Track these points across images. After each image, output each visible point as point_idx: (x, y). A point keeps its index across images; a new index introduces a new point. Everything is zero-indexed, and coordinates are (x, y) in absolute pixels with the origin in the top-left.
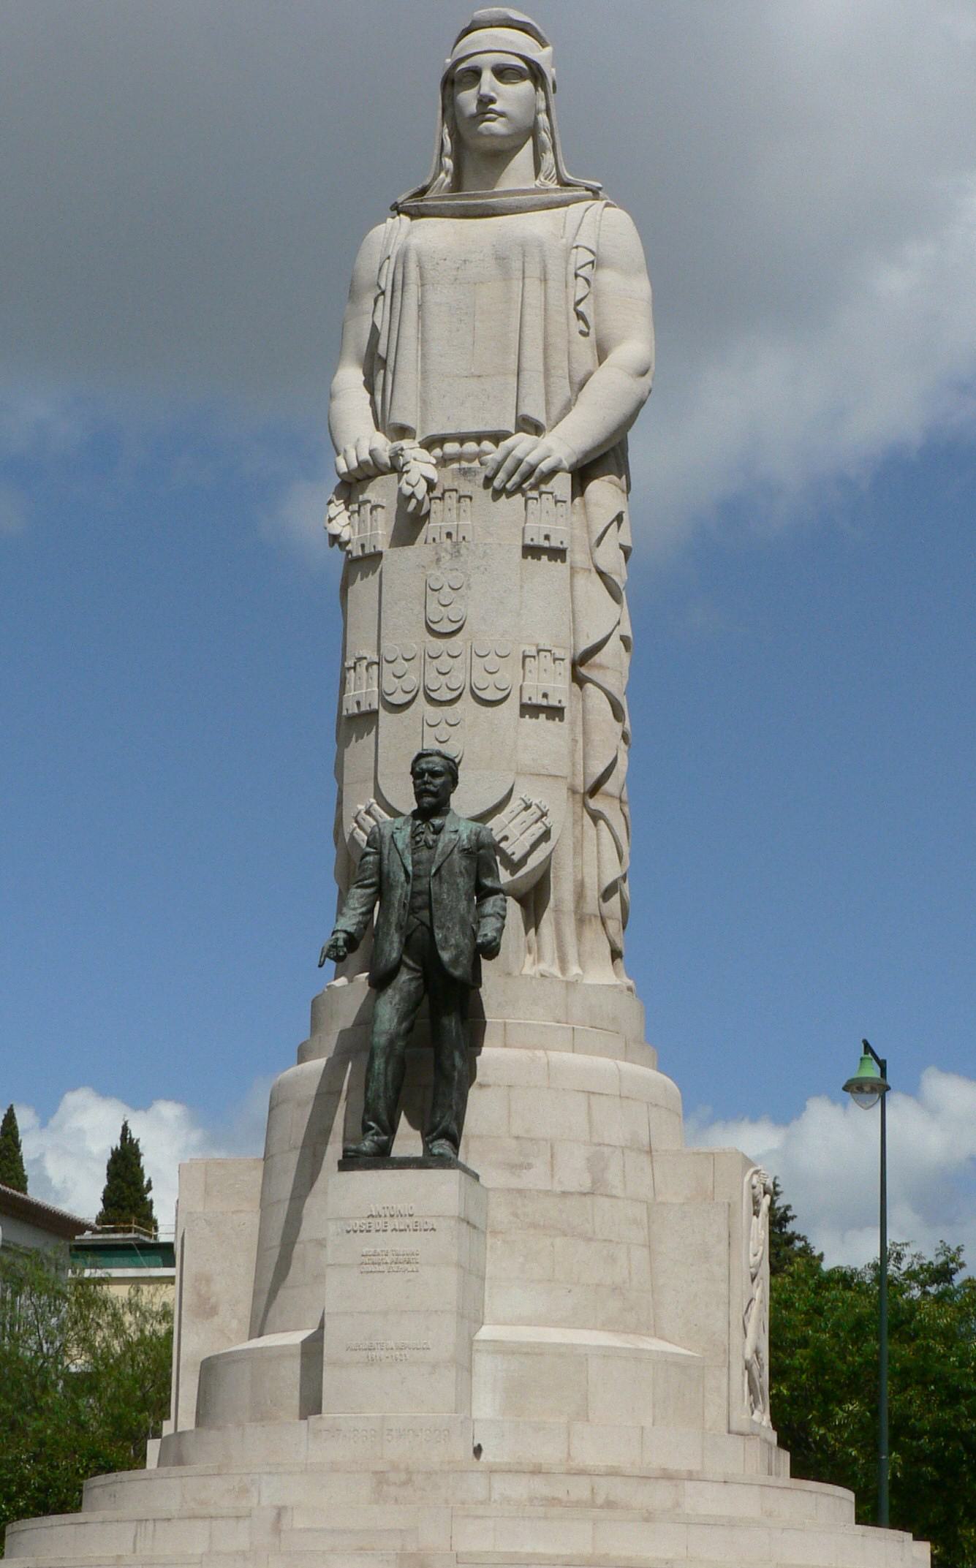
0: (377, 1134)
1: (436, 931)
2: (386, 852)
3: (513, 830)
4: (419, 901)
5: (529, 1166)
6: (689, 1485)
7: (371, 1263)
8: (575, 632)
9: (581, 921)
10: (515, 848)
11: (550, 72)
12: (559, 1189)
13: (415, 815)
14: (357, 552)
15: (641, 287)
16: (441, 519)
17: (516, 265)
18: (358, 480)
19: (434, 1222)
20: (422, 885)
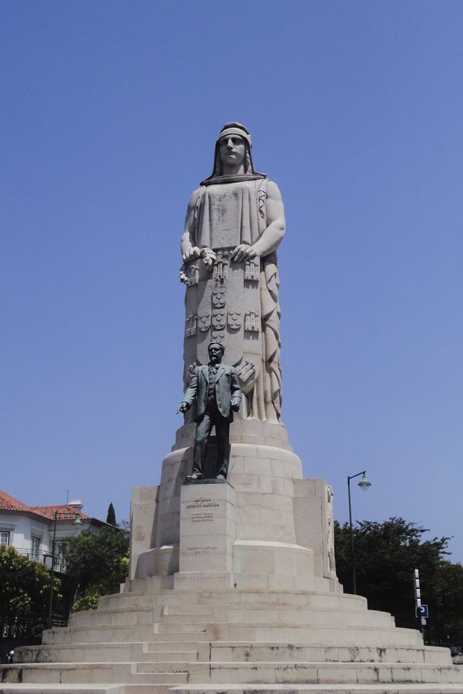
3: (243, 371)
4: (211, 391)
6: (312, 596)
7: (196, 519)
9: (266, 403)
10: (245, 377)
11: (250, 142)
12: (262, 492)
13: (209, 364)
14: (190, 284)
15: (281, 204)
16: (217, 272)
17: (240, 195)
18: (190, 262)
19: (218, 503)
20: (211, 387)
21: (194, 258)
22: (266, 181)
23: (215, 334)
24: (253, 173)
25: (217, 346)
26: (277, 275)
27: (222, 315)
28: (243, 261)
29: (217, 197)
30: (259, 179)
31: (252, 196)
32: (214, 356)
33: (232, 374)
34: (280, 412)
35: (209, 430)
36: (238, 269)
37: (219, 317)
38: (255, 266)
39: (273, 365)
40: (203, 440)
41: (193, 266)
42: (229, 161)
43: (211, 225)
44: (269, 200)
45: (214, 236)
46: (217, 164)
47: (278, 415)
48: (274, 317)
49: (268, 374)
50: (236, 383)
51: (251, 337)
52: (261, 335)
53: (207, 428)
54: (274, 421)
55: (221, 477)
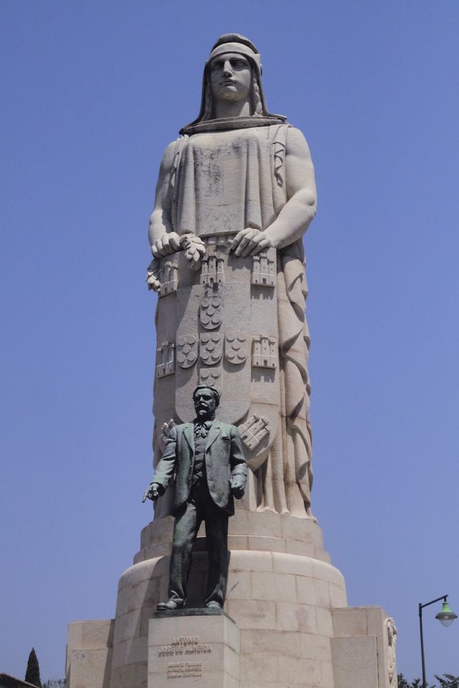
0: (176, 597)
1: (209, 481)
2: (180, 440)
3: (250, 433)
4: (199, 466)
5: (263, 616)
8: (280, 332)
9: (287, 484)
10: (252, 442)
11: (259, 65)
12: (280, 629)
13: (195, 422)
14: (163, 293)
15: (309, 164)
16: (207, 273)
17: (244, 150)
18: (164, 256)
19: (210, 646)
20: (199, 457)
21: (171, 250)
22: (285, 127)
23: (204, 372)
24: (265, 114)
25: (207, 392)
26: (304, 277)
27: (216, 342)
28: (248, 255)
29: (207, 153)
30: (274, 123)
31: (263, 151)
32: (204, 408)
33: (233, 437)
34: (309, 498)
35: (195, 529)
36: (241, 268)
37: (211, 346)
38: (269, 262)
39: (298, 423)
40: (184, 545)
41: (170, 263)
42: (227, 95)
43: (197, 197)
44: (291, 158)
45: (202, 216)
46: (208, 101)
47: (307, 504)
48: (299, 345)
49: (290, 437)
50: (238, 450)
51: (262, 378)
52: (278, 374)
53: (191, 525)
54: (300, 513)
55: (213, 604)
